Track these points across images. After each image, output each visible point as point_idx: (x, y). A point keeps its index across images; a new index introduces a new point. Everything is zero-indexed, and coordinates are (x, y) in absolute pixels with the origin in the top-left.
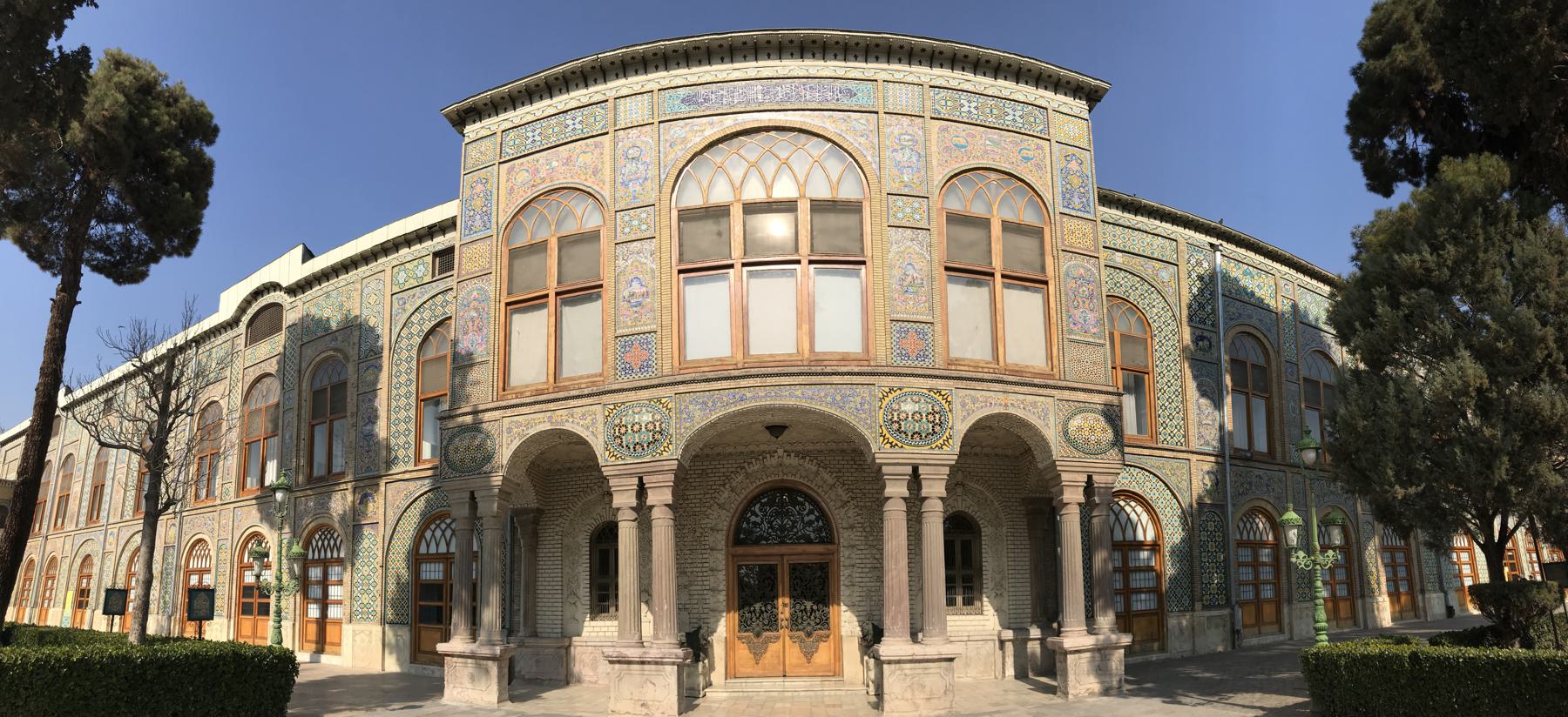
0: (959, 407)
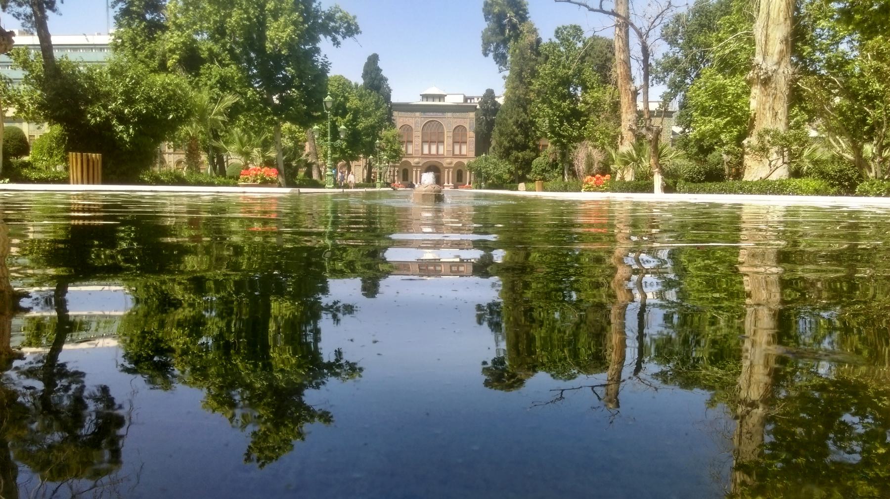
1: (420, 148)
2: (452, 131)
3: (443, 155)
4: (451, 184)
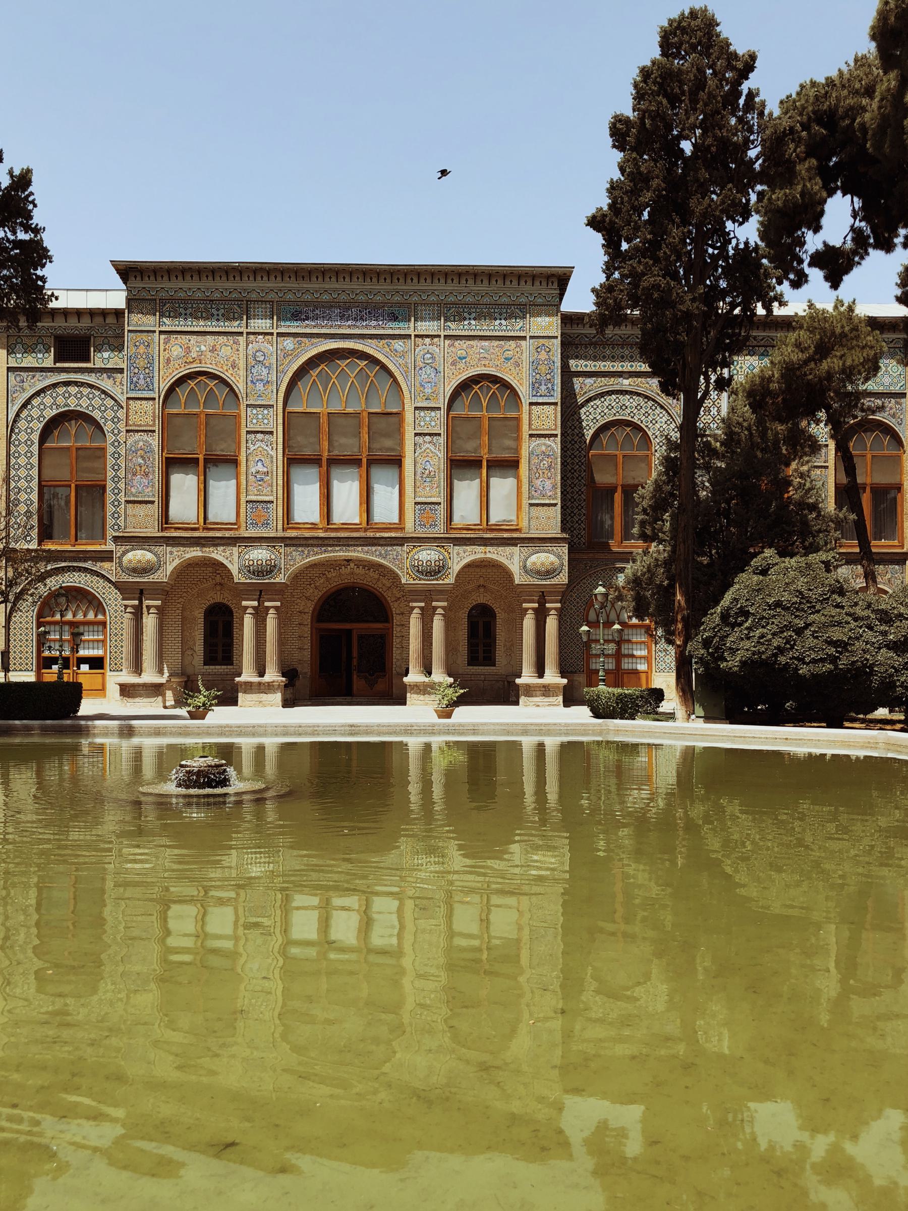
0: (455, 554)
1: (273, 493)
2: (442, 403)
3: (400, 527)
4: (439, 676)
